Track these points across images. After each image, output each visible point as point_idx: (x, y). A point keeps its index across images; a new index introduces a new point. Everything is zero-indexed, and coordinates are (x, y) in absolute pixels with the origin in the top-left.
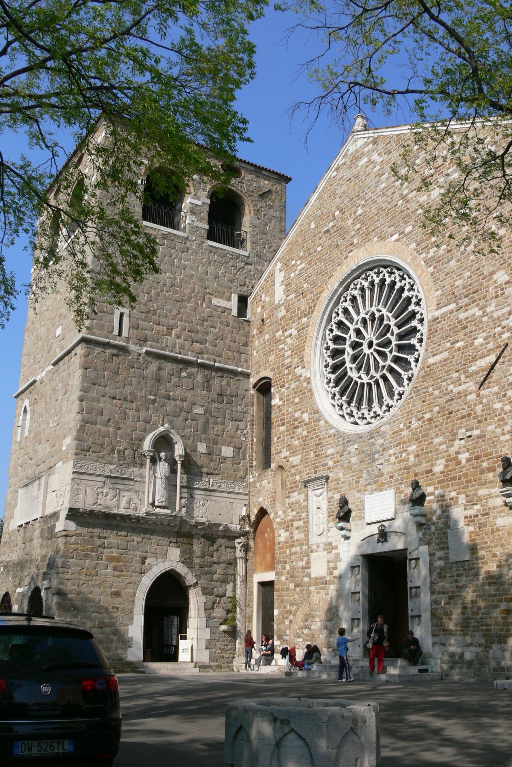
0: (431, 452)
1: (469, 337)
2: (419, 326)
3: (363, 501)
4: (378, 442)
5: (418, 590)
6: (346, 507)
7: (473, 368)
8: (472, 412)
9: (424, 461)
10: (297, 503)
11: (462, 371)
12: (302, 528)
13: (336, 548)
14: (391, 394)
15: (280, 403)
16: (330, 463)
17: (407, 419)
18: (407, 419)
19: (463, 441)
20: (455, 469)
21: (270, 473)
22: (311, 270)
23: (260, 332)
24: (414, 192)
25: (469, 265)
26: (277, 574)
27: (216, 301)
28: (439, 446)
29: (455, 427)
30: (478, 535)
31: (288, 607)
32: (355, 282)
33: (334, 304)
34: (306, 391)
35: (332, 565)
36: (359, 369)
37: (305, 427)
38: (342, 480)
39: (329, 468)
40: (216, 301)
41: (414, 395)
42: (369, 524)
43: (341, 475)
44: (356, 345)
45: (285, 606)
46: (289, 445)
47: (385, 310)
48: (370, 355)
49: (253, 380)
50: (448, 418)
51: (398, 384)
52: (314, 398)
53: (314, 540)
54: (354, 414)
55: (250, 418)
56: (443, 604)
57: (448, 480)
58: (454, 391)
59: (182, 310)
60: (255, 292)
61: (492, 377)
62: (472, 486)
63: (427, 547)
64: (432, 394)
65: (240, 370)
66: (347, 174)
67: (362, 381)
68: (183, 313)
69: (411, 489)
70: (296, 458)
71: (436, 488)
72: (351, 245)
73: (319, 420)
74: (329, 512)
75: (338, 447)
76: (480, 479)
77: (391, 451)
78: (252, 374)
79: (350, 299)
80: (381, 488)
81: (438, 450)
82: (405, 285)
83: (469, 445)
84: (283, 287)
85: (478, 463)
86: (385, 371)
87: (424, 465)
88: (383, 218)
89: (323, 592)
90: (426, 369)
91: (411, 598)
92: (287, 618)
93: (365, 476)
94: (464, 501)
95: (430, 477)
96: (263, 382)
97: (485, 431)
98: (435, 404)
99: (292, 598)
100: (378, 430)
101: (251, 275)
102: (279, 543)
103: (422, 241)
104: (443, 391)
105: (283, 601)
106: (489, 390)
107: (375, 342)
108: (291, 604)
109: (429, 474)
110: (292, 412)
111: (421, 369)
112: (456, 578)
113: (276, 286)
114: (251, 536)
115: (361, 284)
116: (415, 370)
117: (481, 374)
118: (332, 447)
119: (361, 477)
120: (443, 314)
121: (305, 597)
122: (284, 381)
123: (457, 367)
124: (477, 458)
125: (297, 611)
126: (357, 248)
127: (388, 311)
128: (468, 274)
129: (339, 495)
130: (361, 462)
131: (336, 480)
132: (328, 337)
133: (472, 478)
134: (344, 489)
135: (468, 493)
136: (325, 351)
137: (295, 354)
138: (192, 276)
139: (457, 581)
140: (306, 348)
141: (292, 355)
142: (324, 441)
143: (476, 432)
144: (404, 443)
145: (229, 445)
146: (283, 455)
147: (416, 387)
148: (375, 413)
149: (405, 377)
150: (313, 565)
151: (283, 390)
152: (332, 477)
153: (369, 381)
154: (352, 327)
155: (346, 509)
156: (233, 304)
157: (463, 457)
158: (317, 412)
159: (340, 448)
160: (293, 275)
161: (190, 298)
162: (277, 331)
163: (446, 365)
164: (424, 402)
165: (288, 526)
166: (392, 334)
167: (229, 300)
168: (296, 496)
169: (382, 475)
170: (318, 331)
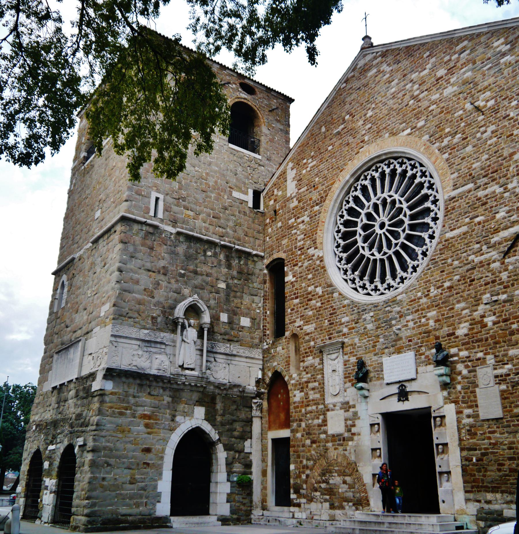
0: (453, 316)
1: (491, 211)
4: (394, 309)
7: (496, 239)
8: (497, 279)
10: (311, 367)
11: (483, 243)
12: (318, 389)
13: (354, 406)
14: (404, 268)
15: (294, 279)
16: (345, 330)
17: (425, 288)
18: (425, 288)
19: (488, 306)
20: (481, 332)
21: (284, 340)
22: (322, 166)
23: (273, 221)
26: (292, 431)
28: (462, 310)
29: (479, 293)
30: (512, 394)
31: (305, 462)
34: (319, 268)
35: (349, 422)
36: (371, 248)
37: (319, 300)
38: (358, 345)
39: (344, 335)
41: (432, 266)
43: (356, 340)
44: (365, 228)
45: (301, 462)
46: (303, 316)
48: (383, 236)
50: (470, 285)
53: (329, 400)
56: (474, 460)
57: (473, 342)
61: (517, 246)
62: (500, 347)
63: (453, 404)
67: (374, 258)
69: (434, 351)
70: (310, 326)
71: (460, 350)
73: (333, 293)
74: (345, 374)
75: (353, 316)
76: (510, 340)
77: (409, 318)
80: (399, 351)
81: (461, 314)
82: (417, 172)
83: (495, 309)
84: (295, 182)
86: (398, 248)
89: (341, 448)
90: (444, 243)
91: (438, 454)
92: (304, 473)
93: (381, 340)
94: (493, 361)
96: (276, 262)
97: (513, 296)
99: (308, 454)
100: (395, 299)
102: (294, 403)
105: (298, 456)
109: (452, 337)
110: (305, 287)
111: (439, 243)
112: (488, 435)
114: (266, 397)
116: (431, 246)
117: (505, 244)
119: (378, 341)
120: (460, 193)
121: (323, 453)
124: (505, 321)
125: (314, 466)
129: (355, 358)
130: (377, 328)
131: (352, 345)
132: (339, 222)
133: (501, 340)
134: (360, 353)
135: (497, 354)
136: (336, 234)
139: (489, 438)
140: (318, 231)
141: (304, 239)
142: (339, 311)
143: (503, 297)
144: (423, 309)
147: (433, 260)
149: (419, 252)
150: (329, 422)
151: (296, 268)
152: (348, 343)
154: (363, 212)
155: (364, 370)
156: (249, 198)
157: (489, 320)
158: (331, 285)
159: (355, 317)
162: (290, 219)
163: (465, 238)
164: (442, 272)
165: (302, 387)
166: (405, 215)
167: (246, 193)
168: (310, 360)
169: (401, 339)
170: (330, 217)
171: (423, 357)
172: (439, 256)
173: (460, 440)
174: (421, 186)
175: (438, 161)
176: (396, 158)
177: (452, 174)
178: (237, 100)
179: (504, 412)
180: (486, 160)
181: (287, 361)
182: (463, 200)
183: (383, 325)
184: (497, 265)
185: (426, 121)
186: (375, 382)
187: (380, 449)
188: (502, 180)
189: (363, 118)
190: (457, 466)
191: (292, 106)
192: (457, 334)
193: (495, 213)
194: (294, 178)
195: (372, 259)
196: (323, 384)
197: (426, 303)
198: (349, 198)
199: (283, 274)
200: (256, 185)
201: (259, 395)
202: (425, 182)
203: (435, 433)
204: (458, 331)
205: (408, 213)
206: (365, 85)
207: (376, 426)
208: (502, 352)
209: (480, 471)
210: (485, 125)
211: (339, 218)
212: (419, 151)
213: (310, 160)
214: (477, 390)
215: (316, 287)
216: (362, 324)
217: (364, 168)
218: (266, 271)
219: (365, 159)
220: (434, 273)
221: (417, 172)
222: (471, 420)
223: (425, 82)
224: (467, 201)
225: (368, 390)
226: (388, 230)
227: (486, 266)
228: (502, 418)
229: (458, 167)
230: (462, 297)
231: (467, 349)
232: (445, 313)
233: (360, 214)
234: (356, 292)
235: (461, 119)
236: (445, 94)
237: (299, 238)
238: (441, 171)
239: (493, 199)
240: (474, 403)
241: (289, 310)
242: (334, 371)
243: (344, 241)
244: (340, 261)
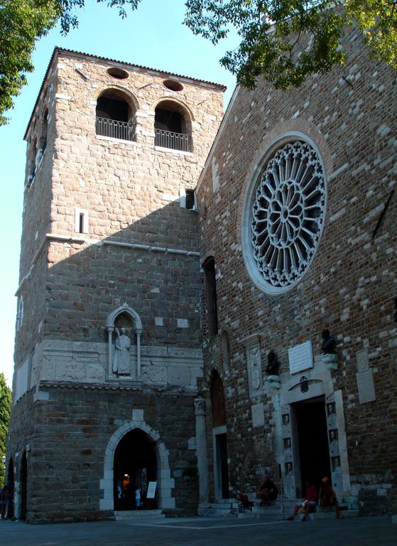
2: (322, 190)
7: (366, 220)
8: (369, 260)
13: (270, 399)
16: (261, 324)
22: (236, 158)
23: (205, 219)
26: (229, 427)
32: (271, 161)
35: (268, 415)
37: (241, 295)
38: (271, 337)
39: (260, 329)
44: (275, 217)
45: (235, 455)
50: (349, 269)
53: (253, 394)
54: (278, 278)
61: (383, 224)
62: (373, 330)
63: (341, 391)
64: (335, 249)
65: (190, 253)
70: (235, 322)
71: (344, 336)
73: (250, 287)
76: (380, 322)
77: (306, 307)
84: (218, 177)
86: (298, 236)
87: (333, 315)
89: (262, 440)
93: (287, 331)
95: (339, 326)
102: (228, 399)
107: (289, 211)
108: (240, 453)
114: (208, 395)
117: (374, 224)
120: (339, 174)
124: (376, 303)
130: (284, 319)
135: (371, 337)
139: (367, 421)
140: (237, 226)
143: (374, 278)
146: (226, 322)
147: (322, 245)
150: (254, 416)
151: (223, 265)
153: (287, 247)
158: (248, 280)
160: (224, 165)
162: (216, 215)
163: (344, 220)
164: (329, 257)
165: (233, 383)
169: (301, 328)
171: (318, 345)
173: (346, 425)
175: (321, 142)
177: (331, 154)
179: (376, 395)
180: (357, 137)
182: (341, 181)
184: (367, 246)
188: (369, 157)
190: (344, 451)
192: (341, 320)
193: (366, 192)
197: (318, 291)
199: (214, 272)
200: (188, 184)
201: (201, 394)
203: (328, 420)
204: (342, 317)
209: (361, 455)
211: (253, 210)
212: (306, 134)
213: (228, 153)
214: (357, 374)
215: (238, 283)
217: (267, 157)
218: (202, 271)
219: (268, 147)
222: (354, 405)
225: (280, 382)
226: (290, 219)
228: (375, 401)
231: (349, 334)
232: (332, 299)
241: (220, 308)
244: (256, 254)
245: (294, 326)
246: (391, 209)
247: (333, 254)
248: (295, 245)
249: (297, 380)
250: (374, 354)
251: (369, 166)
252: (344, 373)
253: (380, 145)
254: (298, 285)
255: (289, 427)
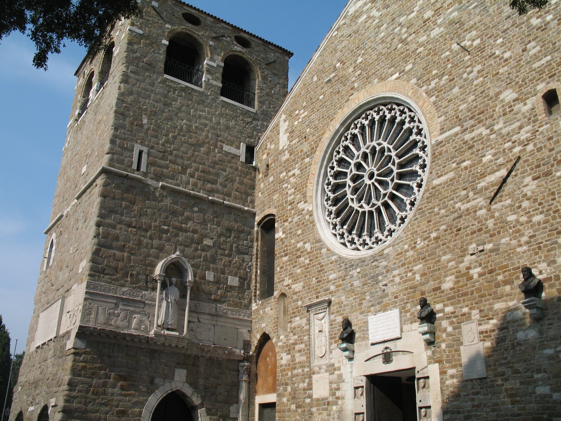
0: (439, 269)
1: (477, 155)
3: (366, 323)
5: (428, 410)
6: (349, 328)
7: (482, 184)
8: (483, 227)
9: (431, 279)
10: (299, 327)
13: (339, 369)
14: (392, 219)
15: (284, 236)
16: (332, 288)
17: (412, 240)
18: (412, 240)
19: (474, 257)
20: (467, 285)
21: (273, 300)
22: (313, 116)
23: (266, 176)
24: (414, 35)
25: (473, 89)
26: (278, 396)
27: (226, 148)
29: (465, 243)
32: (356, 122)
33: (335, 144)
34: (308, 223)
35: (334, 386)
36: (359, 200)
37: (307, 256)
39: (331, 293)
40: (226, 148)
42: (373, 344)
43: (343, 298)
44: (355, 178)
46: (292, 274)
47: (386, 143)
49: (258, 218)
50: (456, 235)
51: (399, 210)
52: (316, 228)
53: (316, 363)
54: (356, 241)
55: (255, 251)
57: (458, 296)
58: (462, 208)
59: (196, 153)
60: (261, 142)
61: (504, 191)
62: (485, 301)
63: (437, 364)
64: (438, 214)
65: (246, 208)
66: (347, 32)
67: (363, 210)
68: (197, 155)
69: (419, 307)
70: (298, 285)
71: (445, 306)
72: (351, 89)
74: (331, 335)
75: (341, 272)
76: (496, 293)
77: (396, 272)
78: (257, 213)
79: (351, 138)
80: (384, 309)
83: (481, 260)
84: (288, 134)
85: (493, 276)
86: (386, 199)
88: (383, 61)
89: (325, 413)
90: (431, 191)
93: (368, 298)
94: (478, 316)
95: (438, 295)
96: (267, 219)
97: (499, 244)
98: (441, 223)
101: (258, 129)
103: (423, 75)
104: (450, 209)
106: (501, 204)
107: (376, 173)
111: (426, 191)
113: (280, 135)
115: (361, 123)
116: (418, 195)
117: (491, 189)
118: (334, 273)
119: (365, 299)
122: (287, 216)
123: (464, 185)
124: (491, 272)
126: (358, 91)
127: (388, 143)
128: (473, 97)
129: (341, 317)
130: (364, 285)
131: (339, 303)
132: (329, 174)
133: (486, 293)
134: (347, 312)
135: (482, 308)
137: (298, 191)
138: (206, 125)
140: (308, 184)
141: (295, 192)
143: (489, 246)
144: (409, 263)
145: (235, 275)
147: (420, 209)
148: (377, 238)
149: (408, 202)
150: (314, 386)
151: (286, 224)
152: (334, 301)
154: (353, 162)
155: (349, 330)
156: (242, 151)
157: (475, 272)
158: (319, 241)
160: (296, 123)
161: (204, 143)
163: (452, 185)
164: (429, 222)
165: (289, 349)
167: (238, 148)
168: (297, 321)
169: (387, 295)
171: (408, 314)
172: (426, 205)
174: (410, 131)
175: (425, 105)
176: (385, 105)
177: (439, 117)
178: (231, 53)
179: (487, 371)
180: (472, 102)
181: (275, 323)
183: (369, 281)
184: (483, 212)
185: (414, 64)
186: (360, 343)
187: (363, 413)
188: (488, 122)
189: (353, 64)
191: (291, 61)
192: (442, 288)
193: (482, 157)
194: (286, 131)
195: (360, 212)
196: (310, 345)
197: (412, 256)
198: (339, 148)
202: (413, 127)
204: (444, 285)
205: (397, 161)
206: (356, 32)
207: (360, 389)
208: (488, 306)
210: (471, 65)
211: (329, 169)
212: (407, 96)
213: (302, 111)
214: (462, 348)
215: (305, 243)
216: (349, 281)
220: (421, 224)
221: (406, 118)
223: (413, 24)
224: (454, 145)
226: (376, 180)
227: (472, 214)
229: (445, 109)
230: (448, 248)
231: (452, 304)
233: (350, 164)
234: (345, 248)
235: (448, 60)
236: (432, 36)
237: (290, 192)
238: (428, 115)
239: (480, 142)
240: (458, 363)
241: (278, 269)
242: (320, 331)
243: (334, 194)
245: (377, 292)
246: (516, 175)
247: (434, 219)
248: (381, 207)
249: (379, 349)
250: (484, 327)
251: (488, 131)
252: (443, 346)
253: (503, 111)
254: (385, 249)
255: (363, 401)
